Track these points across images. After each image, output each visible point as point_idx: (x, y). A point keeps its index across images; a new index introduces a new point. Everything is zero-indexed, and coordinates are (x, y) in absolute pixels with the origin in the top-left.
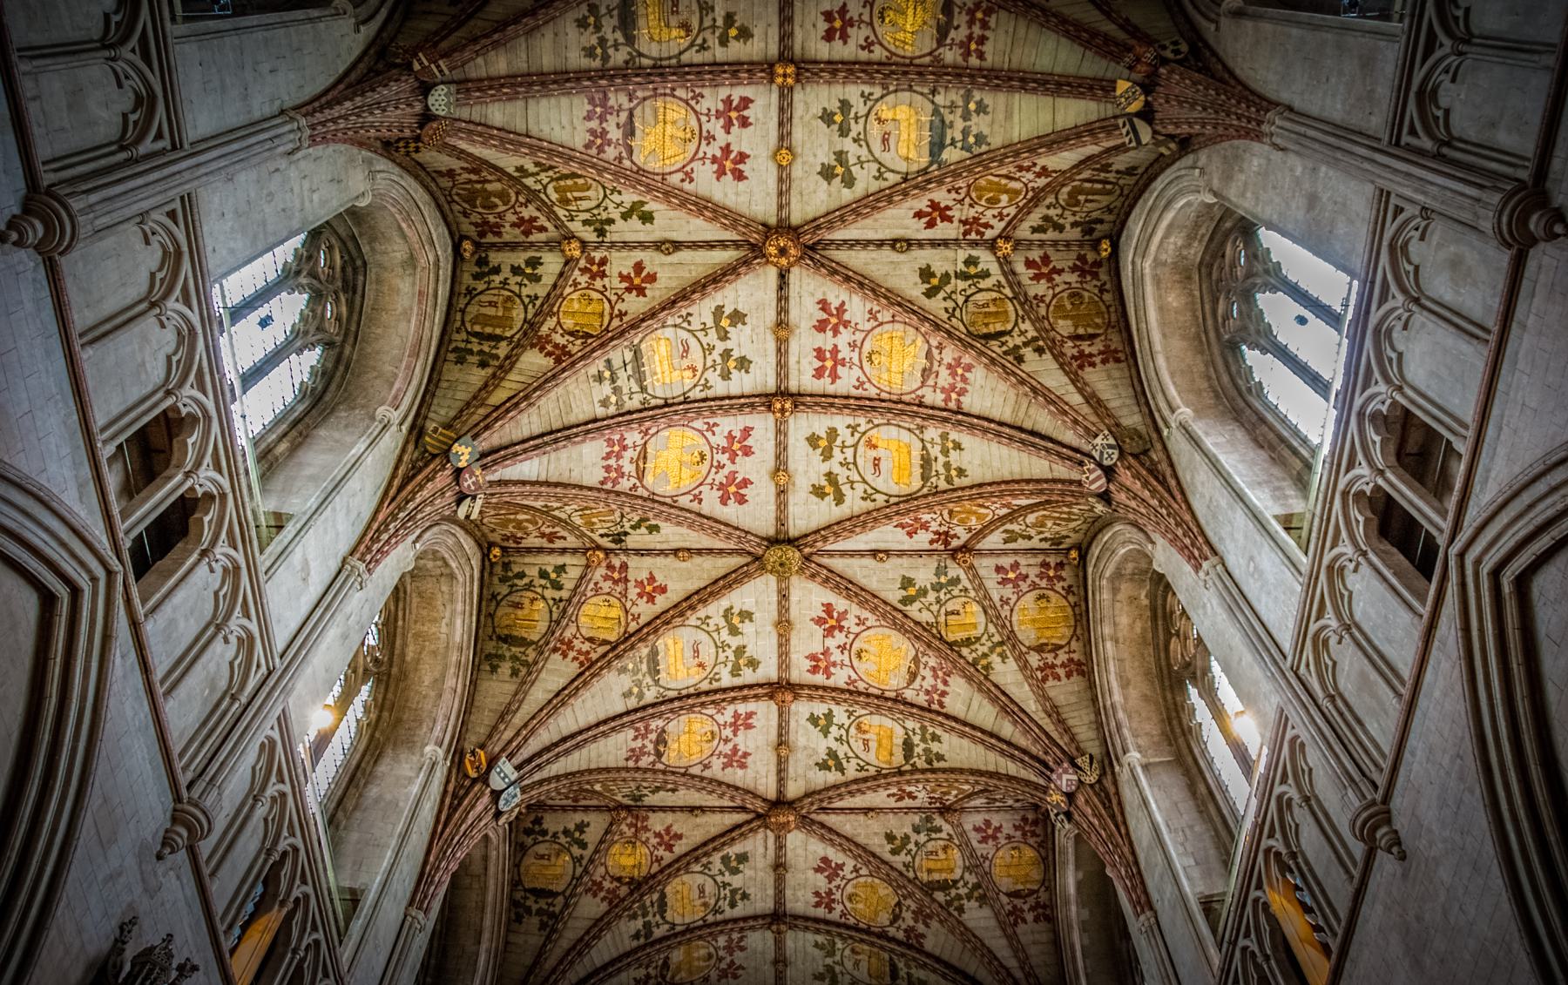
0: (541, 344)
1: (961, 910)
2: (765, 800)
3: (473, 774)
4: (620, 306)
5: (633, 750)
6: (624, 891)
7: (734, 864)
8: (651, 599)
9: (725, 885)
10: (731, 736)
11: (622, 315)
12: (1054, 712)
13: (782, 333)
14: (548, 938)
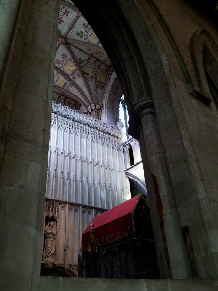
5: (78, 77)
7: (80, 34)
9: (86, 31)
10: (62, 61)
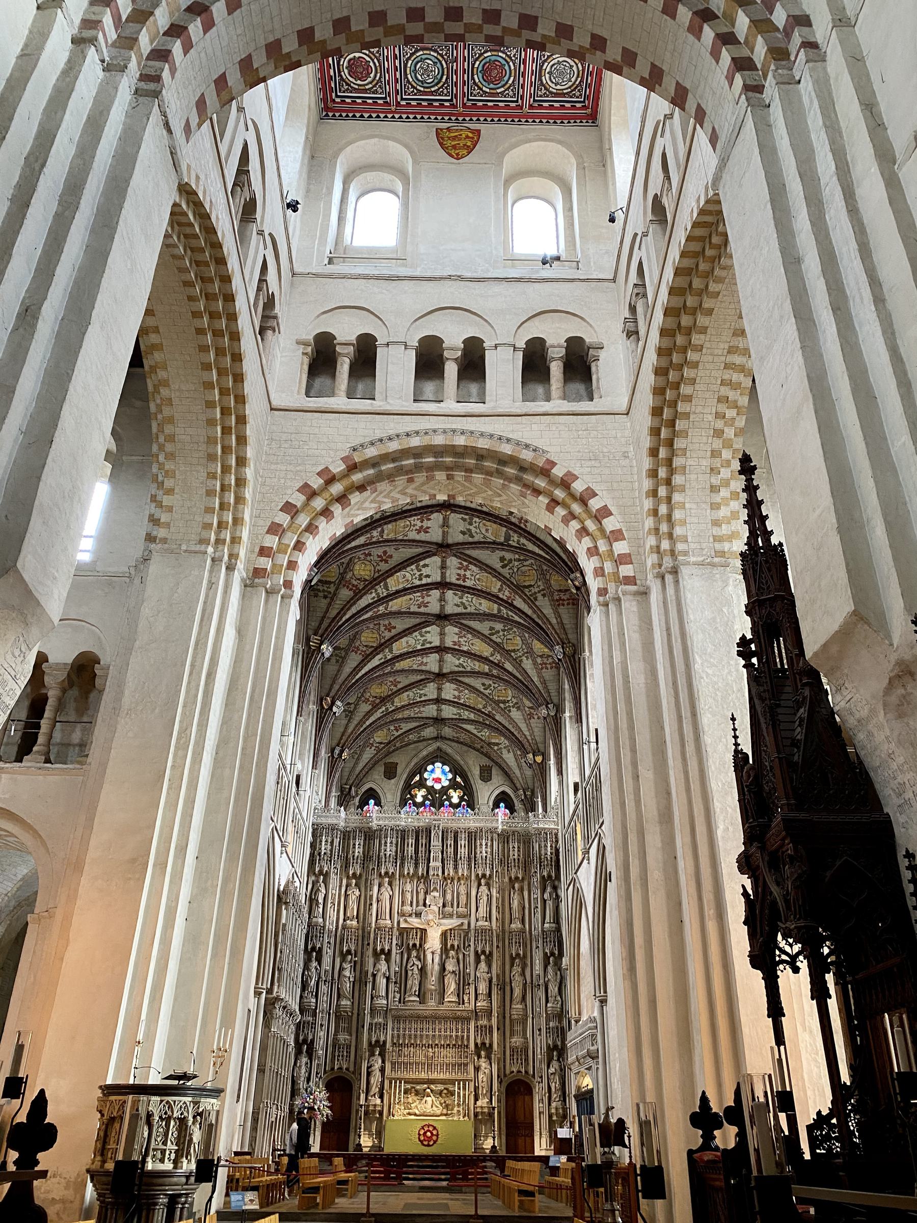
0: (348, 584)
1: (510, 711)
2: (434, 673)
3: (326, 707)
4: (378, 568)
6: (378, 701)
8: (390, 631)
11: (379, 571)
12: (544, 683)
13: (446, 529)
14: (349, 720)
